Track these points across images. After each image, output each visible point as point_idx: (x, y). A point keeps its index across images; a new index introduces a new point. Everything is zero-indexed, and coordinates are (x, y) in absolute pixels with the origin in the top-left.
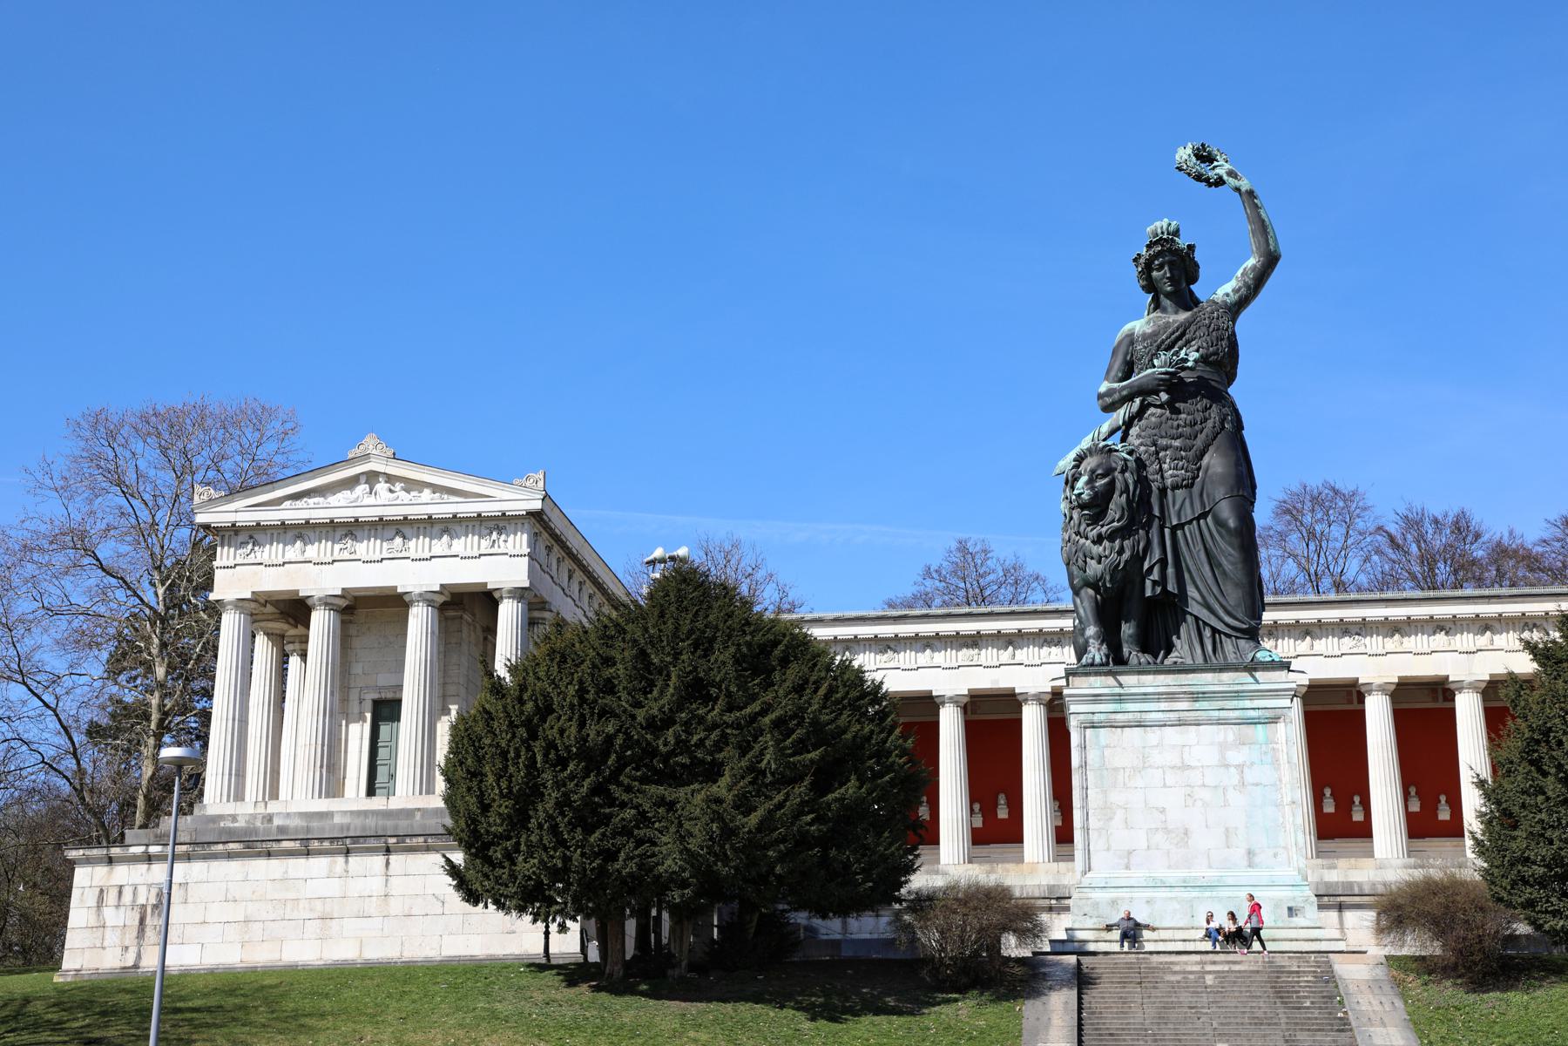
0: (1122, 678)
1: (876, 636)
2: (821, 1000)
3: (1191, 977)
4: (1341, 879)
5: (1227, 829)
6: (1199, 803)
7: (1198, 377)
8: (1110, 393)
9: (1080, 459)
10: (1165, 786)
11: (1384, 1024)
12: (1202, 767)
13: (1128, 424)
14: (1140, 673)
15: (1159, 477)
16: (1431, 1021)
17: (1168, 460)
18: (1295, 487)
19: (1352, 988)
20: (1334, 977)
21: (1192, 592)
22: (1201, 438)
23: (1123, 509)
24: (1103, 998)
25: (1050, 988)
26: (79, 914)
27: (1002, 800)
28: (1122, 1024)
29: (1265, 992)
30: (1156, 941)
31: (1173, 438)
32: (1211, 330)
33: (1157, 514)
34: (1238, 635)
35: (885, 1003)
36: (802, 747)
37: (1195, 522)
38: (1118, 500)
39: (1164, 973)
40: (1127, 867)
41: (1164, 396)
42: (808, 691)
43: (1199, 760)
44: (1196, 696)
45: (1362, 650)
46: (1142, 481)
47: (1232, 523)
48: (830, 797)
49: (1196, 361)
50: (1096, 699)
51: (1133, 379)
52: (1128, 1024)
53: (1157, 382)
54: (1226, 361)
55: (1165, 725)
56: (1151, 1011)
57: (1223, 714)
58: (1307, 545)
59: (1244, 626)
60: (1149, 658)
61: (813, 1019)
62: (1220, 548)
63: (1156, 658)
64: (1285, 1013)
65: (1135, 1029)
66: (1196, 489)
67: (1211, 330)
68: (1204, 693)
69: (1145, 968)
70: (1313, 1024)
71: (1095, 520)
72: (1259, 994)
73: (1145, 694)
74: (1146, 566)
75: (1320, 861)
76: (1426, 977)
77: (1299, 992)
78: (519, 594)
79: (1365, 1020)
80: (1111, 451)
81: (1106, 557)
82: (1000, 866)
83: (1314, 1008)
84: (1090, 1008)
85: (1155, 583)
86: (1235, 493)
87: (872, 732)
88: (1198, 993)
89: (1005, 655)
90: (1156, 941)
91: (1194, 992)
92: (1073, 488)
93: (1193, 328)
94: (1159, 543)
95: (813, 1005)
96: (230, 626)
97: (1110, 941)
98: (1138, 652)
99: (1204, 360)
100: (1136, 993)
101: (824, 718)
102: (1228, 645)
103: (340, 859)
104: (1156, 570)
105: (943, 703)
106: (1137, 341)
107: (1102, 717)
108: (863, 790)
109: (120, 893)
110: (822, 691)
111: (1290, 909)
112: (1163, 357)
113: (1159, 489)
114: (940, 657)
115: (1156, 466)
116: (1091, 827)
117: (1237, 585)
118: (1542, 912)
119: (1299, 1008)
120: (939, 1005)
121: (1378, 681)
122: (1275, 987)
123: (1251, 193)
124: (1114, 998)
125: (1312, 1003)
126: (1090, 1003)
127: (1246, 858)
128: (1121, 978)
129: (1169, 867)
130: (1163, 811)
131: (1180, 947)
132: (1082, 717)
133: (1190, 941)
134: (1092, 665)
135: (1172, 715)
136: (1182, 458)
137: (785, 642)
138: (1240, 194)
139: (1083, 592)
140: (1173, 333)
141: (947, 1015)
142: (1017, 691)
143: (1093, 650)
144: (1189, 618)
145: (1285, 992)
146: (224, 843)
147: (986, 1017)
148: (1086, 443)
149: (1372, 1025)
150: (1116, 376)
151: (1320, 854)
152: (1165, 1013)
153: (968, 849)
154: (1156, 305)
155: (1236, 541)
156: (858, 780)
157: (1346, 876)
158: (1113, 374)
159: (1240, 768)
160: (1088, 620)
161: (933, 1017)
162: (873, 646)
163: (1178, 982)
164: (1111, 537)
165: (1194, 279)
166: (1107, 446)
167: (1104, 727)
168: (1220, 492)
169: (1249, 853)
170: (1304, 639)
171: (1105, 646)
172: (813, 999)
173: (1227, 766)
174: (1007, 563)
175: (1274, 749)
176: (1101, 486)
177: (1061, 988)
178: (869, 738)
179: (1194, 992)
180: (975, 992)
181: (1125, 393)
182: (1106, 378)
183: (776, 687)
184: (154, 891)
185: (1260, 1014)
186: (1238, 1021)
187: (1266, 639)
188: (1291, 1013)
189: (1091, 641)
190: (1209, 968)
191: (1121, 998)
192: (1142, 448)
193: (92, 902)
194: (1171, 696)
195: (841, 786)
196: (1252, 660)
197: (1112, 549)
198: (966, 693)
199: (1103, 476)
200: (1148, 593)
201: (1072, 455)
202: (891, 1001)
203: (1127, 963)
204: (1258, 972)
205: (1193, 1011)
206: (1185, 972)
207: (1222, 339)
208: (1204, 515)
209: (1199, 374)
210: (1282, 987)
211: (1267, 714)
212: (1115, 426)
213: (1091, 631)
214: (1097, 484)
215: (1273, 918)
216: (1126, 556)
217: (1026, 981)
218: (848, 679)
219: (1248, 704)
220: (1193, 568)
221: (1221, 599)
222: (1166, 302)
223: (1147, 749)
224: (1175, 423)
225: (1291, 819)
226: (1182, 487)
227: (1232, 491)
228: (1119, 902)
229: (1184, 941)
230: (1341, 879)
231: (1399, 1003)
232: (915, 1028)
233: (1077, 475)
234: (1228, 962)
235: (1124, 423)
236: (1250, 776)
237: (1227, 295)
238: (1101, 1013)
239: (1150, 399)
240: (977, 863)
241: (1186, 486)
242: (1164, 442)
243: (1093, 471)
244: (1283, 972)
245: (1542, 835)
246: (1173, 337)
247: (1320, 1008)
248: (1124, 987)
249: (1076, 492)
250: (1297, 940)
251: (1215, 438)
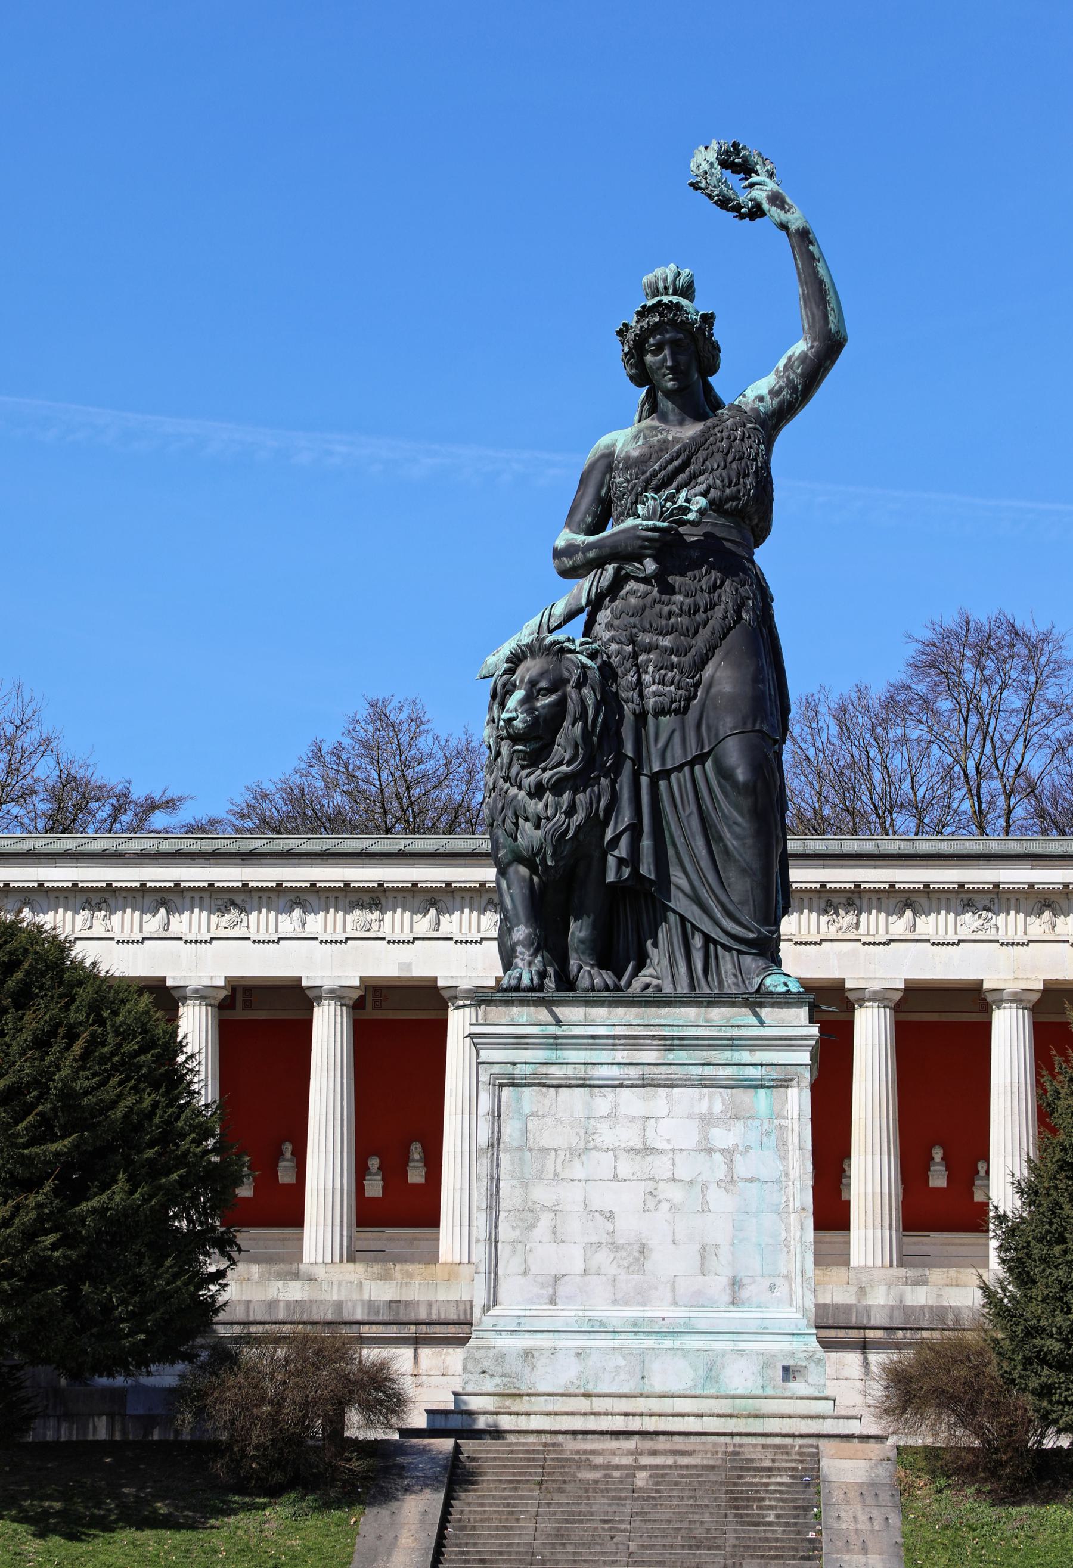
0: (561, 1011)
1: (211, 885)
2: (57, 1505)
3: (617, 1474)
4: (930, 1303)
5: (704, 1247)
6: (665, 1206)
7: (706, 535)
8: (570, 550)
9: (515, 660)
10: (615, 1178)
11: (865, 1550)
12: (673, 1150)
13: (596, 604)
14: (588, 1003)
15: (635, 696)
16: (931, 1545)
17: (651, 669)
18: (951, 620)
19: (837, 1495)
20: (818, 1477)
21: (677, 877)
22: (705, 634)
23: (577, 745)
24: (482, 1505)
25: (407, 1490)
27: (416, 1152)
28: (501, 1545)
29: (716, 1499)
30: (584, 1414)
31: (660, 634)
32: (730, 458)
33: (630, 754)
34: (742, 948)
35: (155, 1511)
36: (44, 1132)
37: (686, 769)
38: (570, 731)
39: (579, 1468)
40: (552, 1301)
41: (650, 566)
42: (55, 1048)
43: (669, 1141)
44: (669, 1043)
45: (991, 934)
46: (610, 701)
47: (741, 775)
48: (84, 1206)
49: (701, 512)
50: (520, 1041)
51: (608, 532)
52: (509, 1545)
53: (639, 542)
54: (751, 510)
55: (621, 1086)
56: (547, 1525)
57: (709, 1071)
58: (966, 722)
59: (751, 936)
60: (608, 977)
61: (41, 1535)
62: (722, 811)
63: (619, 977)
64: (736, 1531)
65: (517, 1553)
66: (692, 716)
67: (730, 458)
68: (681, 1038)
69: (552, 1459)
70: (770, 1548)
71: (533, 760)
72: (706, 1502)
73: (593, 1037)
74: (609, 835)
75: (902, 1271)
76: (943, 1481)
77: (763, 1499)
79: (840, 1544)
80: (563, 651)
81: (548, 819)
82: (398, 1267)
83: (778, 1524)
84: (460, 1520)
85: (621, 861)
86: (749, 727)
87: (155, 1105)
88: (620, 1499)
89: (423, 924)
90: (584, 1414)
91: (614, 1498)
92: (502, 705)
93: (702, 454)
94: (630, 800)
95: (46, 1513)
97: (517, 1414)
98: (592, 966)
99: (716, 506)
100: (531, 1498)
101: (80, 1085)
102: (727, 963)
104: (624, 841)
105: (319, 999)
106: (617, 468)
107: (528, 1070)
108: (137, 1195)
110: (78, 1047)
111: (786, 1369)
112: (651, 502)
113: (634, 713)
114: (316, 923)
115: (632, 677)
116: (501, 1238)
117: (743, 871)
118: (1059, 1402)
119: (757, 1524)
120: (236, 1514)
121: (1013, 986)
122: (732, 1492)
123: (804, 237)
124: (498, 1505)
125: (778, 1516)
126: (461, 1512)
127: (728, 1291)
128: (514, 1474)
129: (615, 1302)
130: (611, 1216)
131: (619, 1424)
132: (496, 1069)
133: (634, 1415)
134: (517, 988)
135: (632, 1071)
136: (672, 667)
137: (26, 966)
138: (788, 234)
139: (511, 870)
140: (671, 461)
141: (247, 1531)
142: (440, 983)
143: (520, 964)
144: (672, 917)
145: (743, 1499)
147: (303, 1534)
148: (525, 636)
149: (848, 1551)
150: (583, 520)
151: (904, 1259)
152: (567, 1529)
153: (350, 1238)
154: (652, 407)
155: (746, 803)
156: (128, 1181)
157: (939, 1296)
158: (578, 517)
159: (729, 1154)
160: (517, 915)
161: (225, 1532)
162: (207, 901)
163: (596, 1482)
164: (558, 787)
165: (713, 369)
166: (557, 642)
167: (529, 1085)
168: (727, 724)
169: (734, 1284)
170: (901, 914)
171: (539, 958)
172: (47, 1504)
173: (710, 1151)
174: (454, 742)
175: (780, 1127)
176: (544, 707)
177: (421, 1491)
178: (152, 1114)
179: (614, 1498)
180: (293, 1495)
181: (591, 554)
182: (568, 524)
183: (7, 1039)
185: (699, 1532)
186: (668, 1541)
187: (842, 912)
188: (744, 1531)
189: (520, 949)
190: (645, 1461)
191: (508, 1505)
192: (614, 647)
195: (102, 1191)
196: (758, 990)
197: (557, 806)
198: (357, 983)
199: (549, 691)
200: (611, 878)
201: (507, 649)
202: (162, 1508)
203: (528, 1452)
204: (713, 1468)
205: (606, 1526)
206: (608, 1467)
207: (746, 476)
208: (701, 759)
209: (708, 529)
210: (742, 1492)
211: (774, 1073)
212: (574, 607)
213: (521, 932)
214: (539, 704)
215: (760, 1382)
216: (578, 818)
217: (373, 1479)
218: (123, 1023)
219: (746, 1057)
220: (680, 841)
221: (719, 892)
222: (666, 405)
223: (592, 1121)
224: (666, 609)
225: (798, 1234)
226: (669, 712)
227: (745, 723)
228: (536, 1354)
229: (626, 1414)
230: (932, 1302)
231: (895, 1520)
232: (196, 1551)
233: (509, 687)
234: (674, 1453)
235: (588, 603)
236: (742, 1168)
237: (761, 399)
238: (474, 1528)
239: (628, 568)
240: (362, 1261)
241: (677, 712)
242: (646, 638)
243: (533, 683)
244: (748, 1469)
245: (1061, 1299)
246: (670, 467)
247: (787, 1524)
248: (516, 1489)
249: (505, 715)
250: (790, 1417)
251: (725, 635)
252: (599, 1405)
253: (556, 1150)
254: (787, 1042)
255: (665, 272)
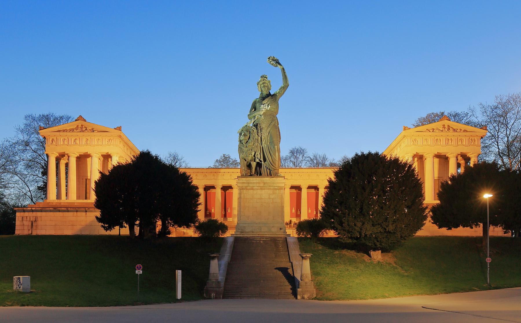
3: (258, 241)
10: (257, 202)
26: (18, 223)
103: (76, 213)
107: (245, 187)
109: (27, 218)
111: (280, 228)
132: (240, 187)
135: (259, 187)
146: (49, 208)
184: (34, 218)
193: (21, 220)
194: (259, 183)
252: (254, 233)
253: (249, 198)
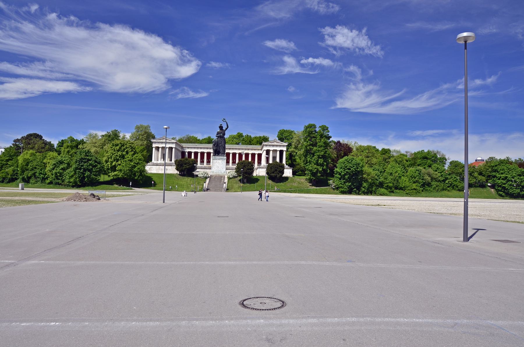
38: (216, 144)
46: (218, 143)
78: (174, 148)
96: (154, 149)
254: (225, 158)
255: (221, 124)
